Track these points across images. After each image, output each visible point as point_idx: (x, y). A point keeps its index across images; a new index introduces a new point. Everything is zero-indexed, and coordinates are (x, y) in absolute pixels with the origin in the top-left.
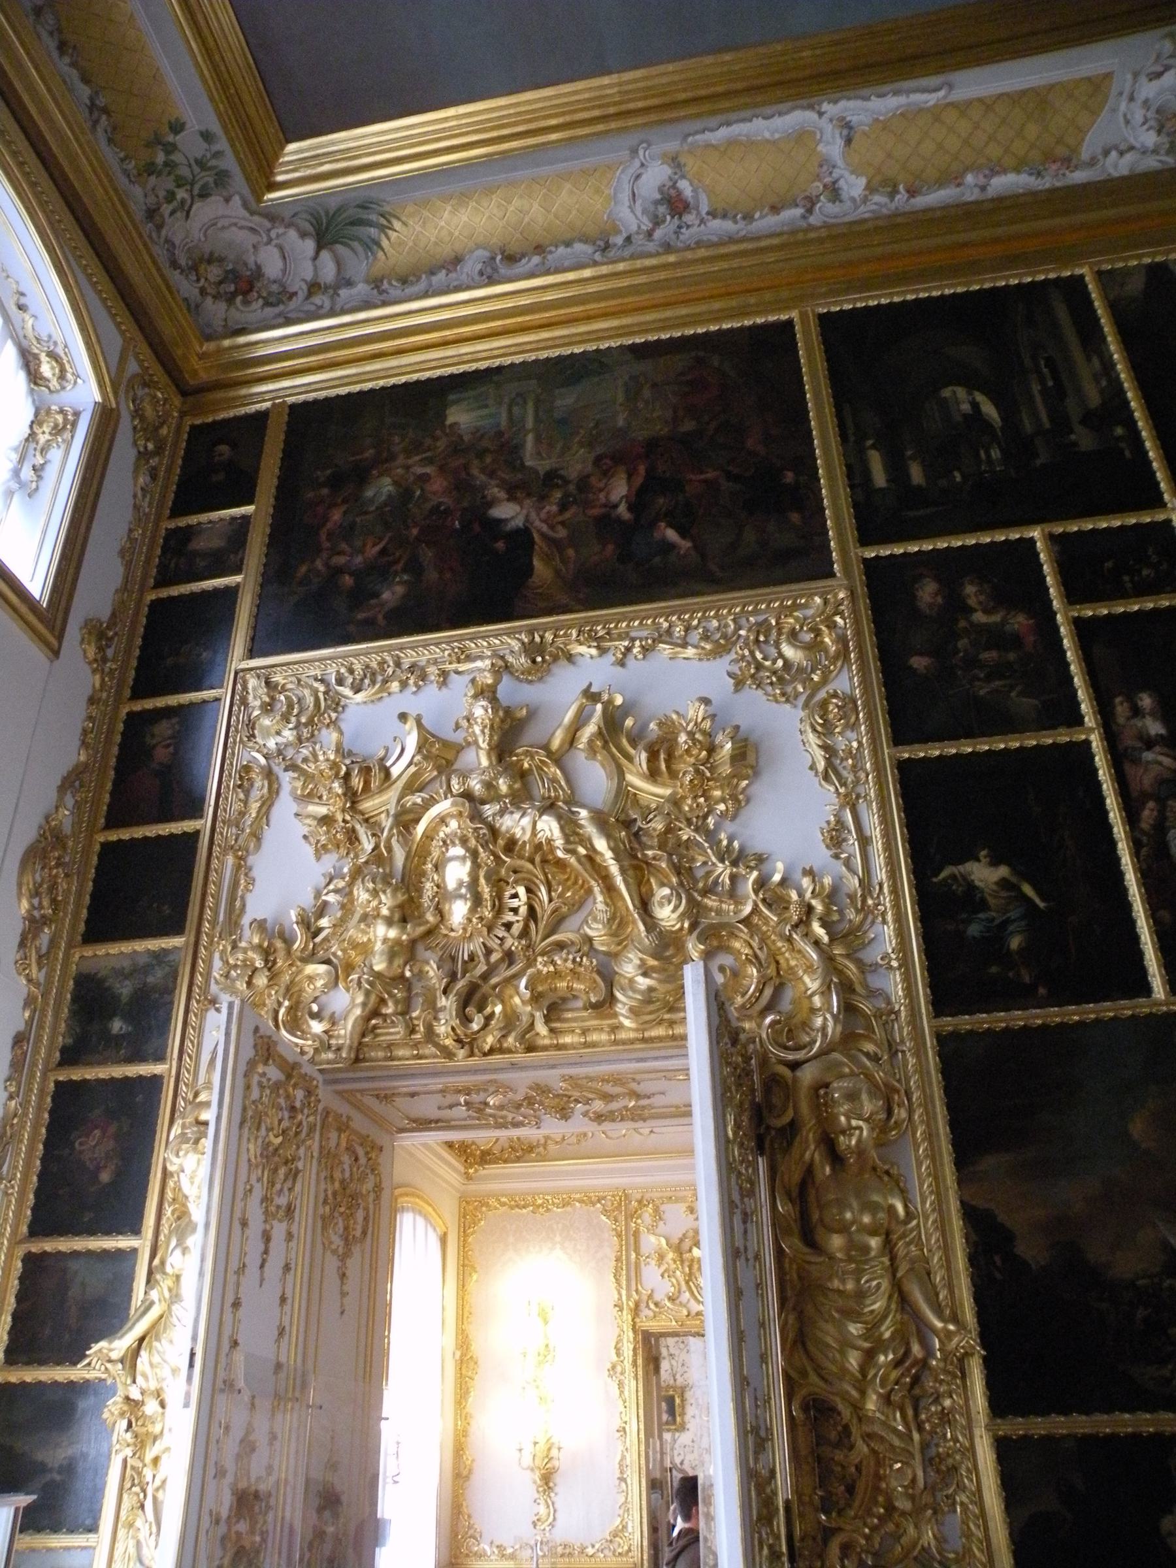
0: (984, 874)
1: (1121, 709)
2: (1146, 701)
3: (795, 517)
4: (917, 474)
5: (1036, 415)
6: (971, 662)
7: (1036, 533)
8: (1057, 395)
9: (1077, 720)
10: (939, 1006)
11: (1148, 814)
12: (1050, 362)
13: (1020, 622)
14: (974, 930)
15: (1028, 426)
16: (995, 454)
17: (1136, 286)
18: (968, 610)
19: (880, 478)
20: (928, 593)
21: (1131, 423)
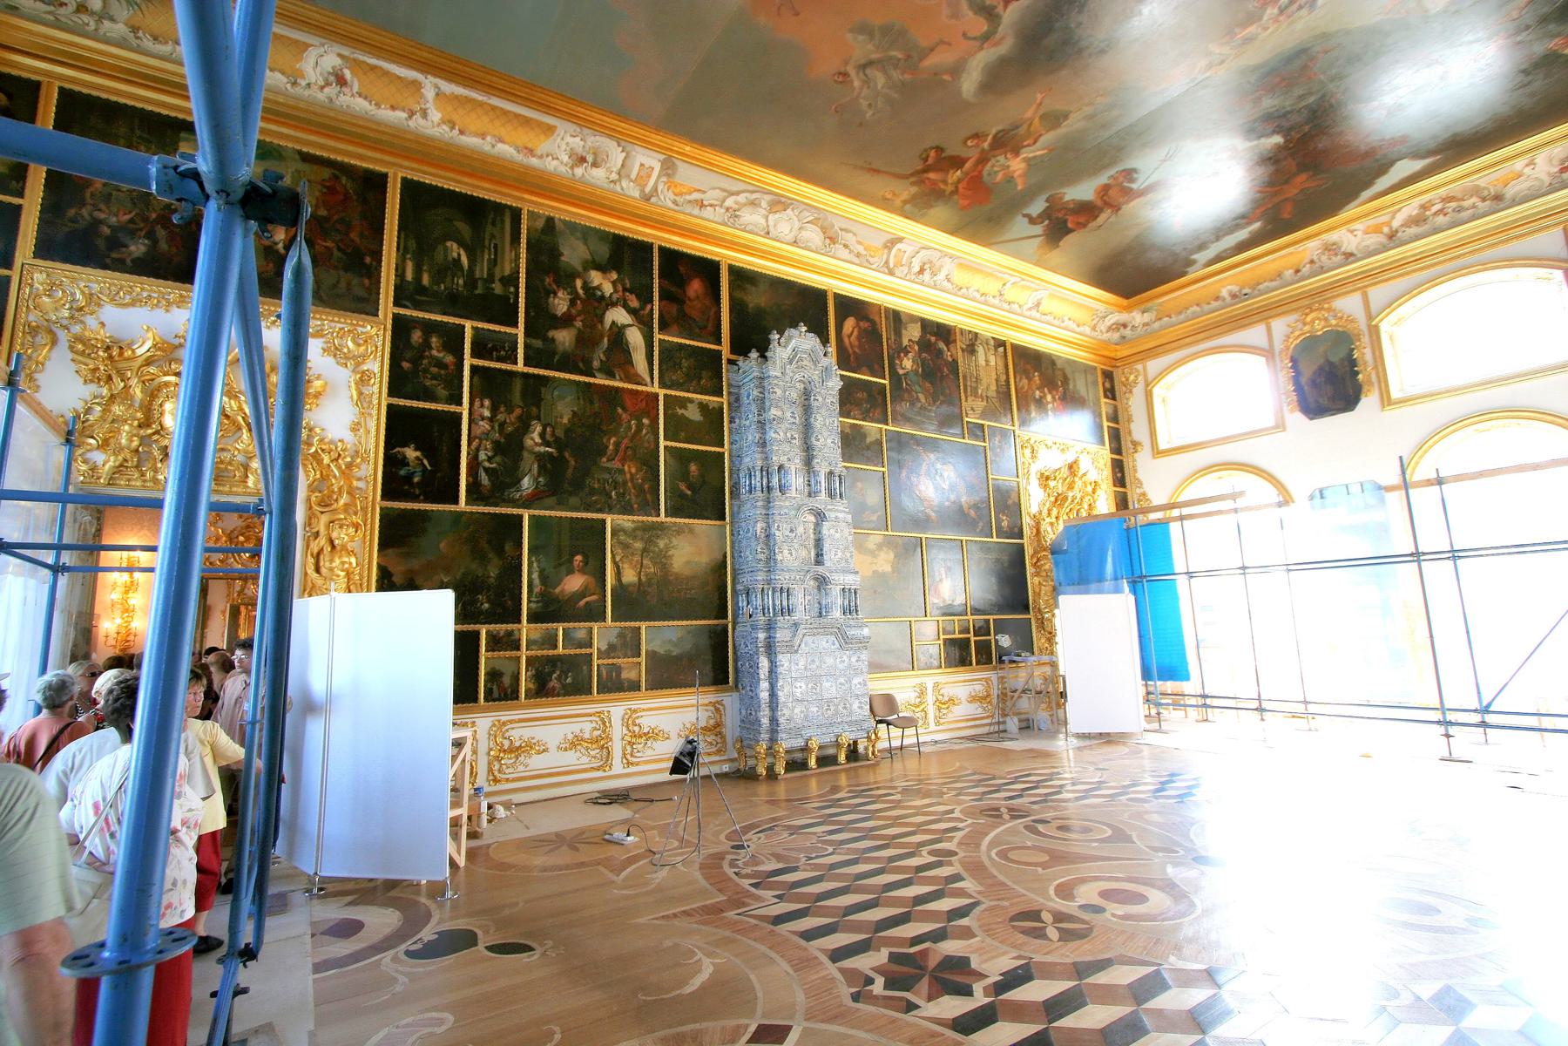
0: (411, 453)
1: (477, 403)
2: (487, 402)
3: (366, 281)
4: (426, 280)
5: (482, 271)
6: (426, 371)
7: (468, 325)
8: (494, 263)
9: (460, 404)
10: (385, 496)
11: (475, 444)
12: (496, 246)
13: (449, 359)
14: (402, 473)
15: (478, 275)
16: (461, 282)
17: (540, 224)
18: (431, 348)
19: (409, 276)
20: (416, 336)
21: (517, 288)
